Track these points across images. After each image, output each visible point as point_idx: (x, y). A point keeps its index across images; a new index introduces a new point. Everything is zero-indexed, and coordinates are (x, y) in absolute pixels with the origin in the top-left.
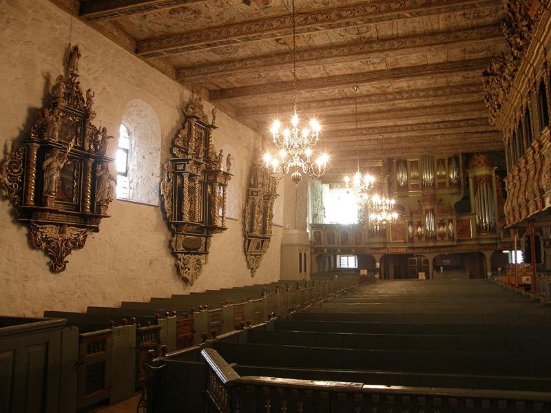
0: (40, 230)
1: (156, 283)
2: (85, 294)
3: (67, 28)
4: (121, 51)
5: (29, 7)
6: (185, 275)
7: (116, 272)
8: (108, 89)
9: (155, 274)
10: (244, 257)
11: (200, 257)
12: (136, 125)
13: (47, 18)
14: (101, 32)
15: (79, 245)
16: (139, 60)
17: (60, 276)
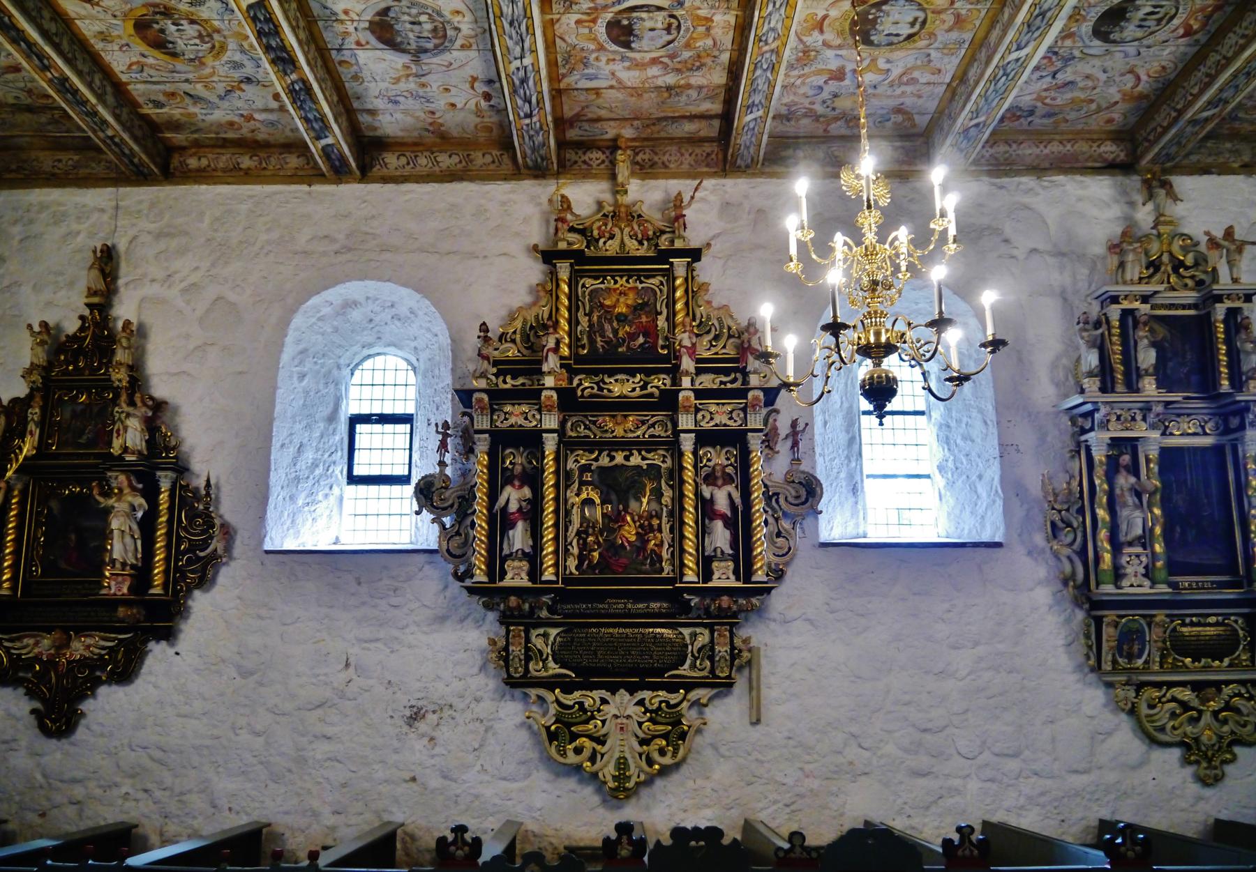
0: (6, 644)
1: (445, 777)
2: (146, 791)
3: (105, 217)
4: (275, 193)
5: (15, 222)
6: (572, 758)
7: (261, 740)
8: (232, 297)
9: (438, 750)
10: (1094, 697)
11: (674, 698)
12: (413, 344)
13: (55, 223)
14: (200, 183)
15: (124, 668)
16: (342, 187)
17: (74, 744)
